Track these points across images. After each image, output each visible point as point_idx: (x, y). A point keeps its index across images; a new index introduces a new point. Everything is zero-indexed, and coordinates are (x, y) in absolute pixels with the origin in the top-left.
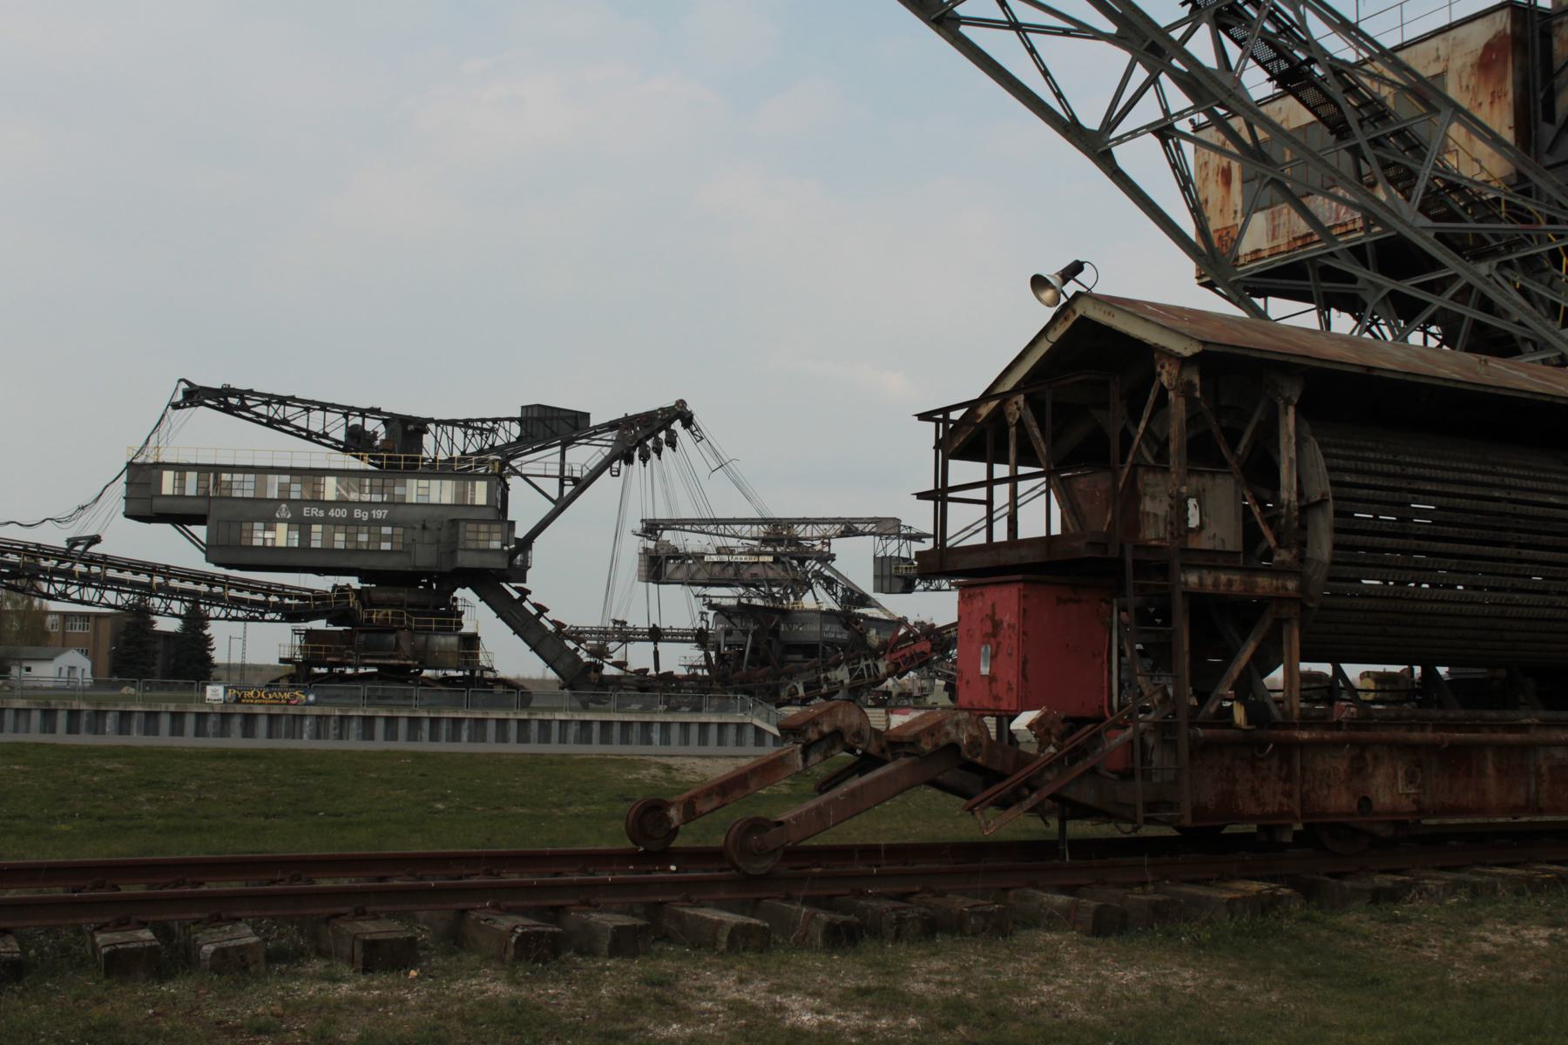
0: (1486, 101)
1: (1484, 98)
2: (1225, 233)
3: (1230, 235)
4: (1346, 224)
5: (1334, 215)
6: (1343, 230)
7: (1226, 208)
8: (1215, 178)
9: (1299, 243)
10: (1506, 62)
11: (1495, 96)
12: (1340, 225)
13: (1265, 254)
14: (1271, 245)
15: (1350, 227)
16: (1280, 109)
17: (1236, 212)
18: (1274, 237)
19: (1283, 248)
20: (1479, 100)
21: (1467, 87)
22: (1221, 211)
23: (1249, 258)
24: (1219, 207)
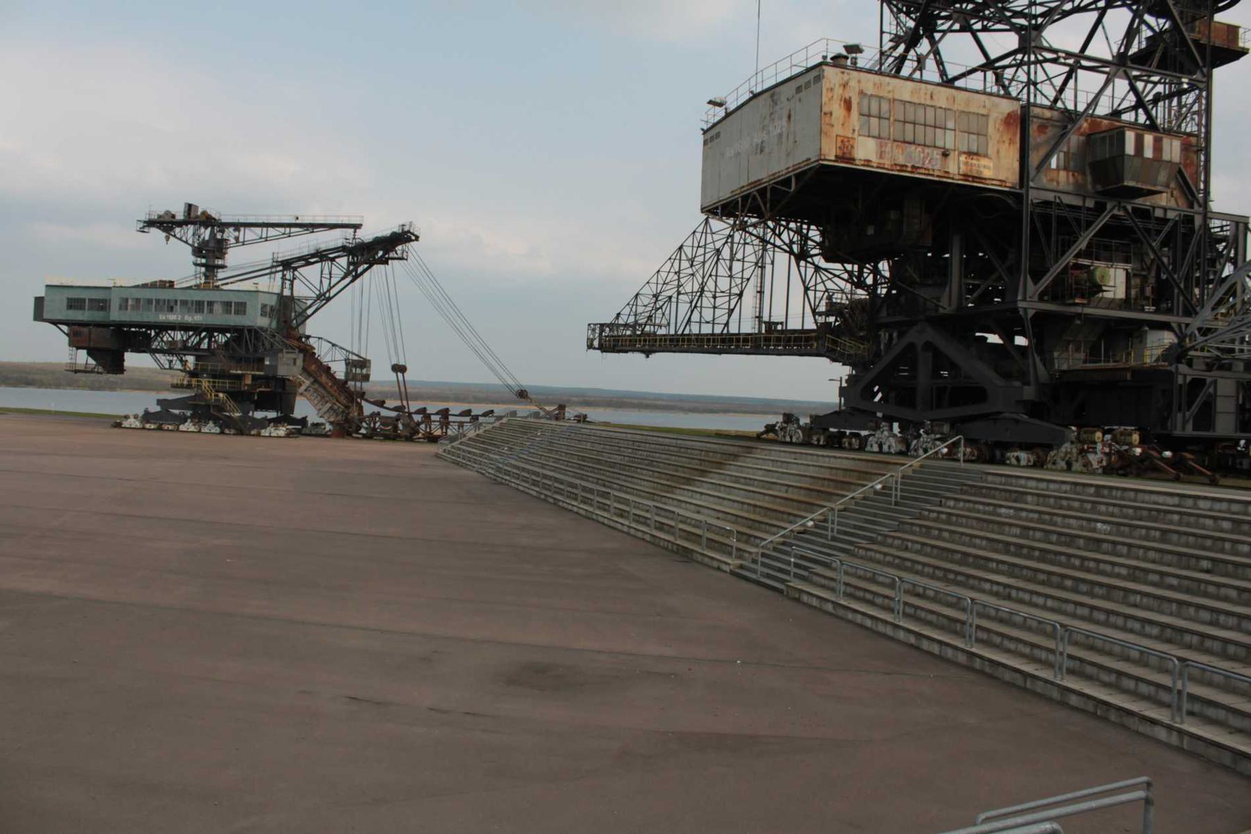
0: (1007, 142)
1: (1006, 138)
2: (846, 140)
3: (851, 143)
4: (928, 170)
5: (921, 162)
6: (927, 172)
7: (846, 124)
8: (838, 102)
9: (898, 168)
10: (1017, 126)
11: (1011, 142)
12: (925, 169)
13: (875, 165)
14: (878, 161)
15: (931, 172)
16: (888, 83)
17: (854, 130)
18: (881, 157)
19: (886, 167)
20: (1004, 139)
21: (998, 130)
22: (843, 125)
23: (863, 163)
24: (841, 123)
